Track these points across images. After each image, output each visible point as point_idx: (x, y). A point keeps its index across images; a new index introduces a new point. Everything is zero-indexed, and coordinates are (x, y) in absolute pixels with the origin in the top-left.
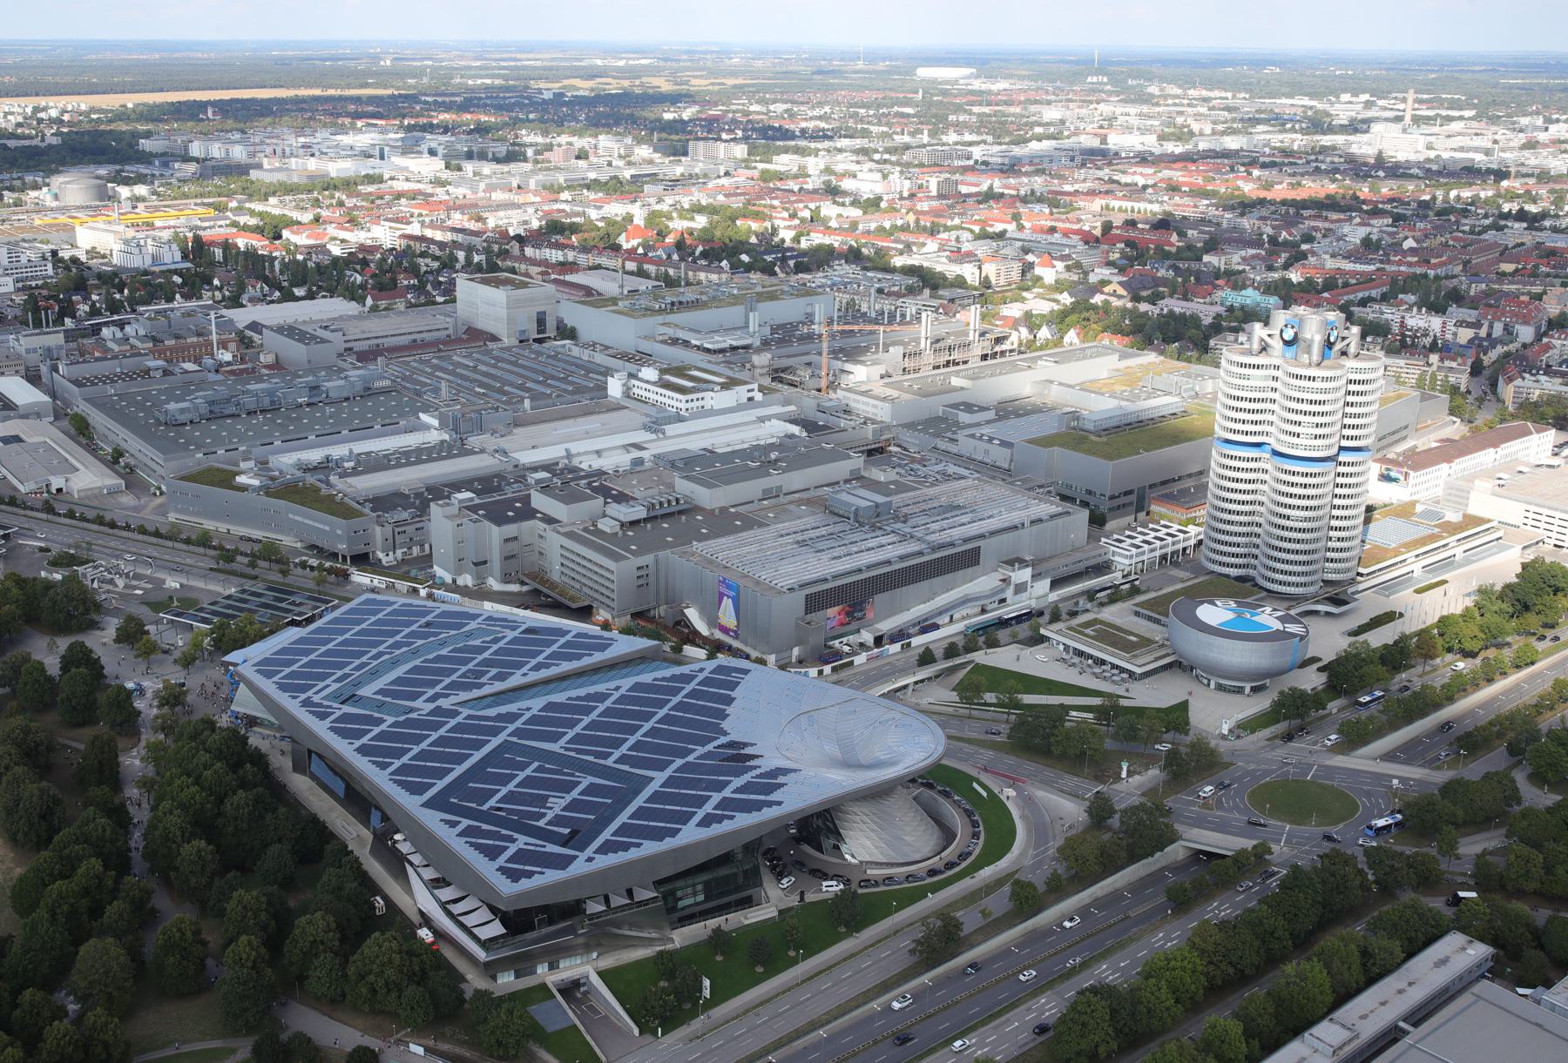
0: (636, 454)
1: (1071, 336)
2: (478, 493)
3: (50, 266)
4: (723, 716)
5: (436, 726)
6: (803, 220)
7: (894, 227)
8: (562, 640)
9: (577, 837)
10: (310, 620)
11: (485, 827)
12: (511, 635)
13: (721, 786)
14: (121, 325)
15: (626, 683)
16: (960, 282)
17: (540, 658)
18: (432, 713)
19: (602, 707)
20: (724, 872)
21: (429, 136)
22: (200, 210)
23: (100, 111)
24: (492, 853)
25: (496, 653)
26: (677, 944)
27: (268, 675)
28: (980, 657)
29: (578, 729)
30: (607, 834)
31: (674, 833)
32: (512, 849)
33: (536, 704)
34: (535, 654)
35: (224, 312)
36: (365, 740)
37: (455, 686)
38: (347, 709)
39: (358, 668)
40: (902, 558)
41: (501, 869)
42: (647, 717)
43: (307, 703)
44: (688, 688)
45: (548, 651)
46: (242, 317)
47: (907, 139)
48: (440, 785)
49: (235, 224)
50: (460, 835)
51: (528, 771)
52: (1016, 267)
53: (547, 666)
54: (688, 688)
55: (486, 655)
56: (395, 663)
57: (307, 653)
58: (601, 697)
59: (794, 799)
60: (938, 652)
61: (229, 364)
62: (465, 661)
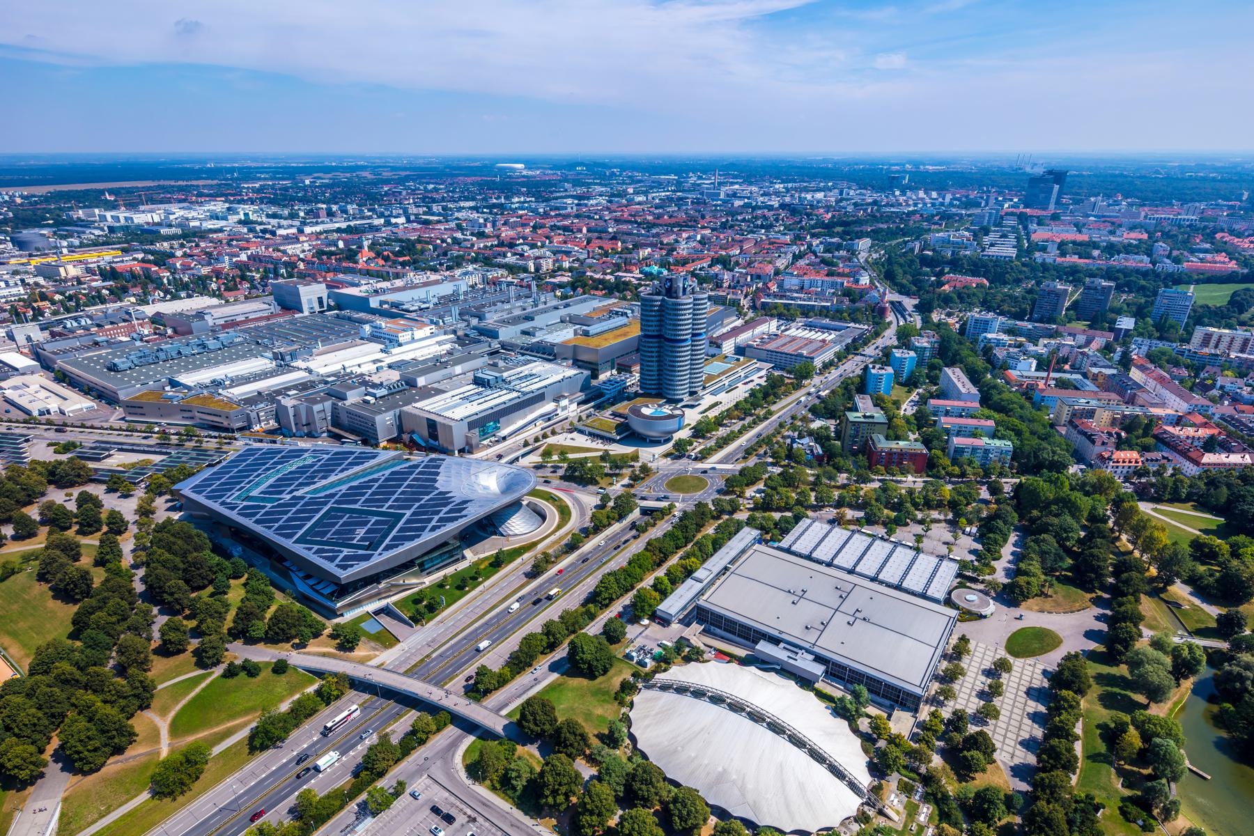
0: (379, 364)
1: (580, 290)
2: (300, 390)
3: (21, 288)
4: (436, 481)
5: (294, 505)
6: (448, 244)
7: (492, 245)
8: (353, 456)
9: (373, 546)
10: (220, 462)
11: (326, 547)
12: (326, 457)
13: (438, 512)
14: (75, 319)
15: (387, 472)
16: (525, 270)
17: (343, 466)
18: (292, 499)
19: (377, 485)
20: (445, 549)
21: (242, 206)
22: (112, 252)
23: (35, 196)
24: (332, 559)
25: (321, 466)
26: (427, 583)
27: (199, 493)
28: (551, 440)
29: (366, 496)
30: (387, 541)
31: (418, 536)
32: (342, 556)
33: (344, 488)
34: (340, 465)
35: (138, 308)
36: (258, 517)
37: (301, 485)
38: (245, 503)
39: (248, 483)
40: (510, 400)
41: (337, 566)
42: (400, 486)
43: (223, 503)
44: (417, 471)
45: (347, 462)
46: (150, 310)
47: (495, 201)
48: (301, 532)
49: (135, 259)
50: (314, 553)
51: (345, 519)
52: (550, 261)
53: (347, 469)
54: (417, 471)
55: (315, 468)
56: (268, 478)
57: (219, 479)
58: (376, 480)
59: (474, 513)
60: (531, 441)
61: (147, 336)
62: (305, 472)
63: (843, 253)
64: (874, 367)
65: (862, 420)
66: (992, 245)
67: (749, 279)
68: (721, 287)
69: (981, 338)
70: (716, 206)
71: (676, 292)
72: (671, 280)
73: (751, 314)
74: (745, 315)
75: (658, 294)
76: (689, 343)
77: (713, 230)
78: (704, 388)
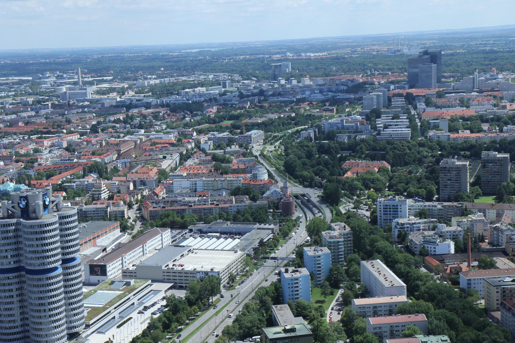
63: (235, 148)
64: (287, 271)
65: (283, 335)
66: (386, 127)
67: (132, 187)
68: (99, 199)
69: (393, 224)
70: (83, 107)
71: (34, 212)
72: (26, 198)
73: (138, 226)
74: (132, 228)
75: (10, 217)
76: (60, 271)
77: (82, 134)
78: (88, 326)
